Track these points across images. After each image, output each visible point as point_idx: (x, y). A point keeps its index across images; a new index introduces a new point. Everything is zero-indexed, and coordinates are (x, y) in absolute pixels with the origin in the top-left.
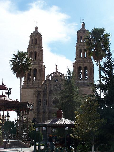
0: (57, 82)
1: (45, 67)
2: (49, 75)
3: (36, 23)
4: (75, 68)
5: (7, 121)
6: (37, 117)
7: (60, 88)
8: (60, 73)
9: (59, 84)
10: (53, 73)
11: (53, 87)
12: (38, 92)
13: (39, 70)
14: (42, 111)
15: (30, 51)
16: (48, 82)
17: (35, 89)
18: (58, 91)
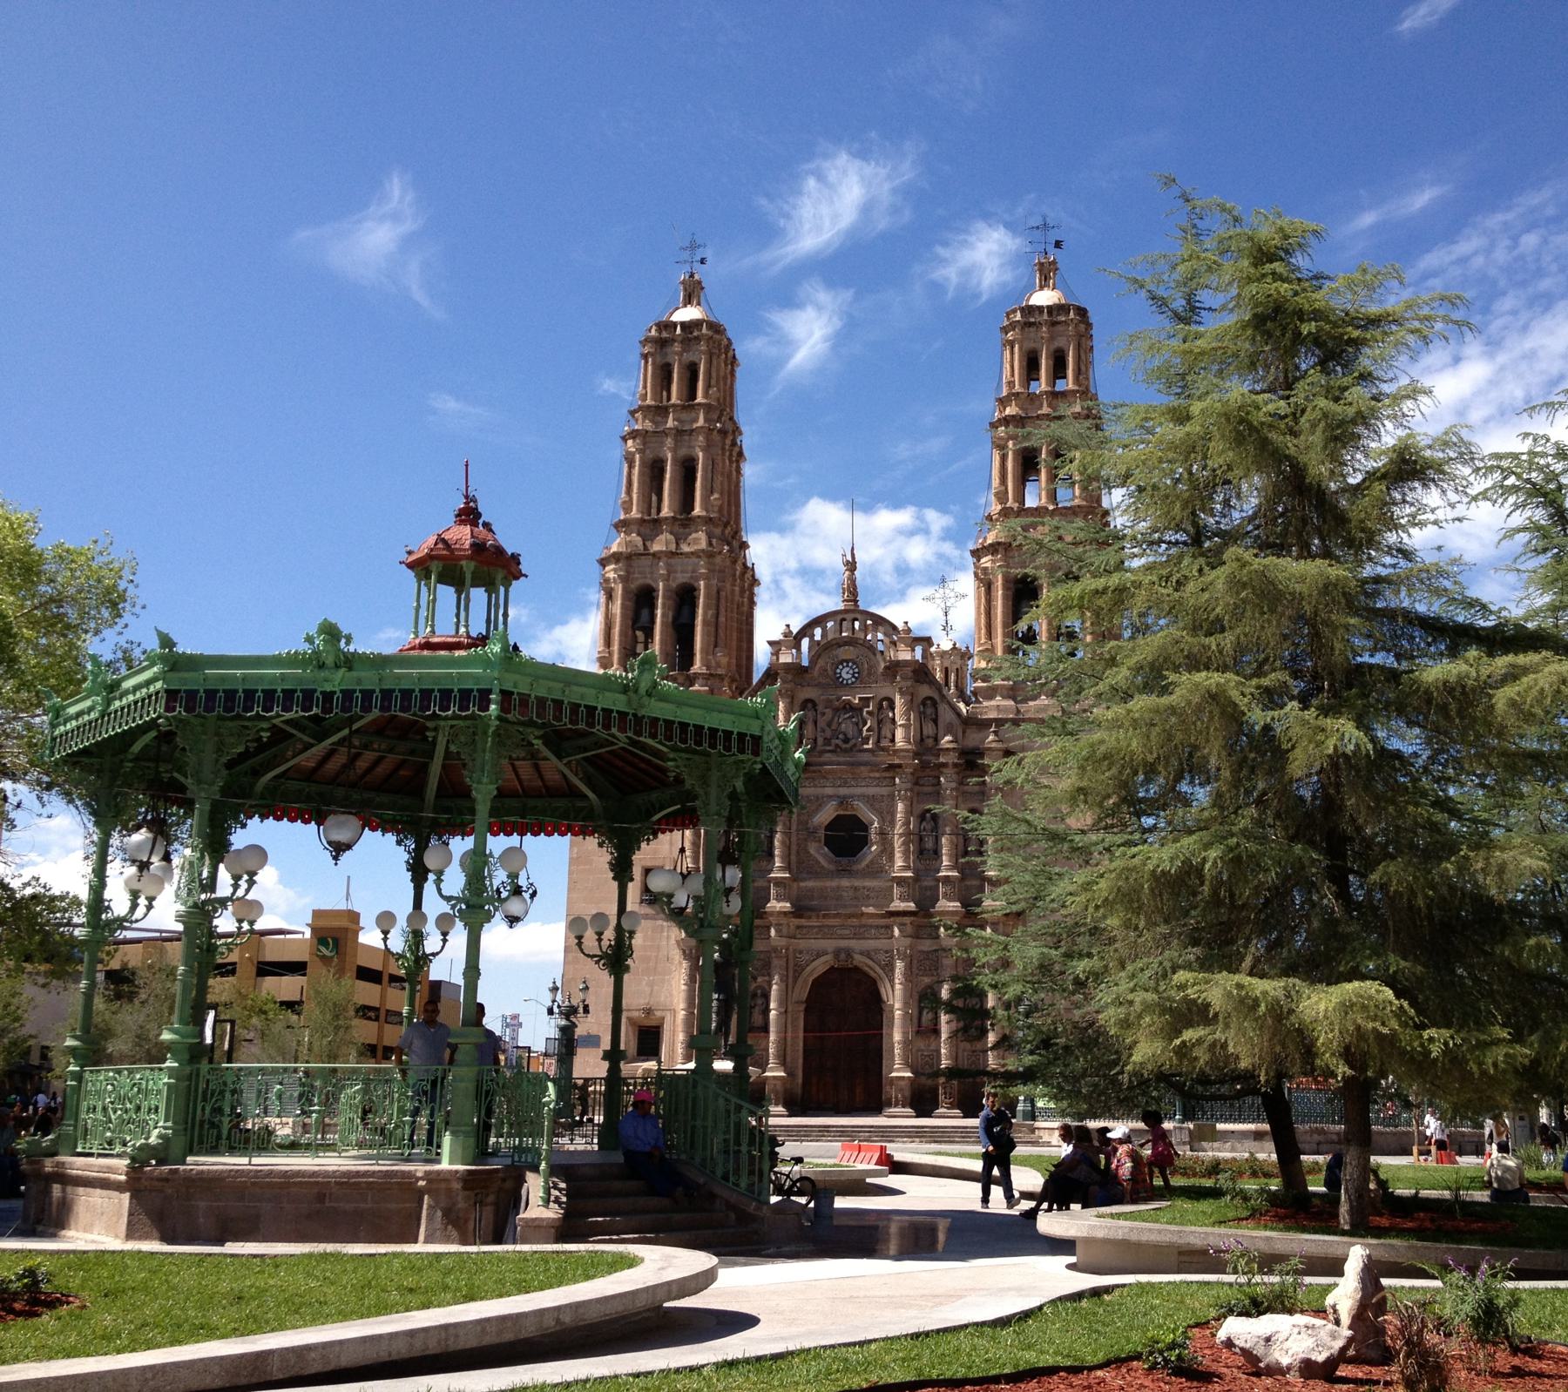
1: (758, 576)
2: (795, 630)
9: (865, 701)
10: (819, 621)
13: (718, 592)
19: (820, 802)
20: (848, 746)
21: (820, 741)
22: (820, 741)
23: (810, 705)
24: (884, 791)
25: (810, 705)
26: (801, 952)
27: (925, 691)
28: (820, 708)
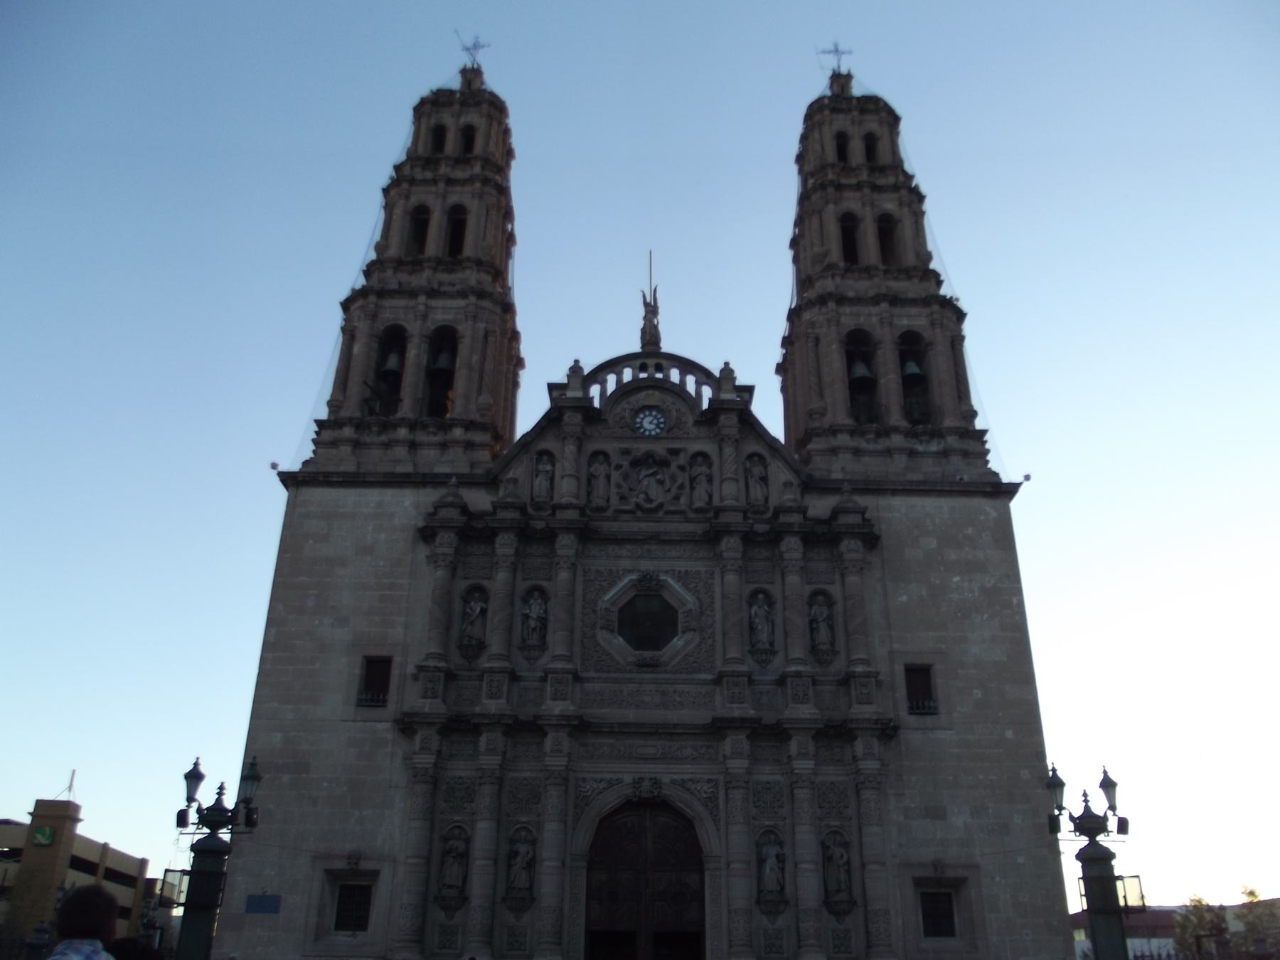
0: (657, 438)
2: (587, 369)
3: (476, 46)
4: (817, 340)
5: (158, 891)
6: (435, 765)
7: (692, 488)
8: (688, 366)
9: (675, 452)
10: (614, 365)
11: (615, 476)
12: (464, 509)
13: (486, 337)
14: (503, 701)
15: (414, 200)
16: (573, 420)
17: (429, 496)
18: (668, 512)
19: (613, 578)
20: (653, 505)
21: (614, 500)
22: (614, 500)
23: (601, 457)
24: (700, 567)
25: (601, 457)
26: (584, 780)
27: (752, 447)
28: (615, 459)
